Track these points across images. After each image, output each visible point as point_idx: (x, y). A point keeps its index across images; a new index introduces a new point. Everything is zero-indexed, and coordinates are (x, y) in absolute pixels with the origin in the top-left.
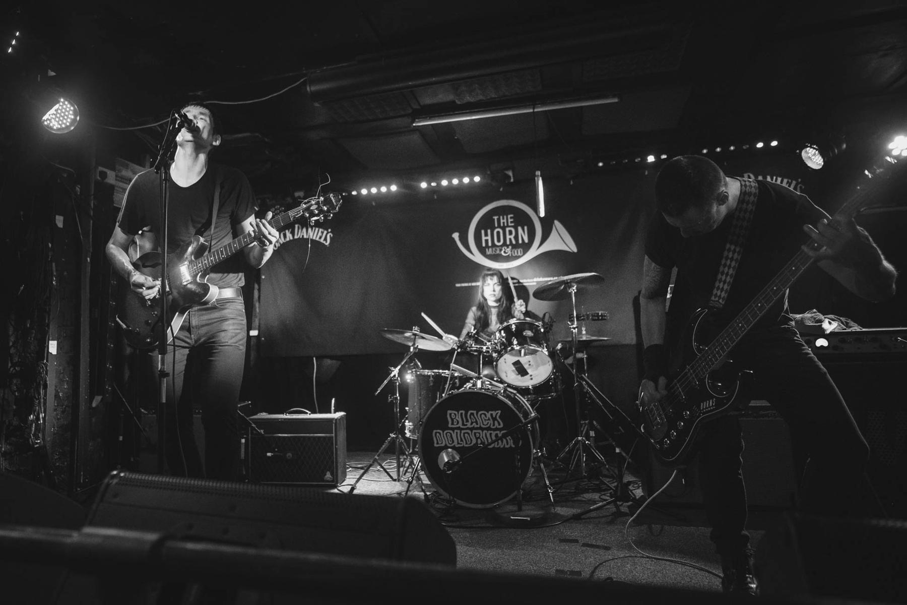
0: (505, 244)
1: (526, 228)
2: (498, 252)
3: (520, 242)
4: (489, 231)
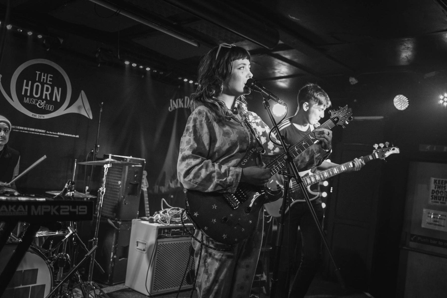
0: (41, 98)
1: (60, 89)
2: (34, 103)
3: (54, 99)
4: (30, 82)
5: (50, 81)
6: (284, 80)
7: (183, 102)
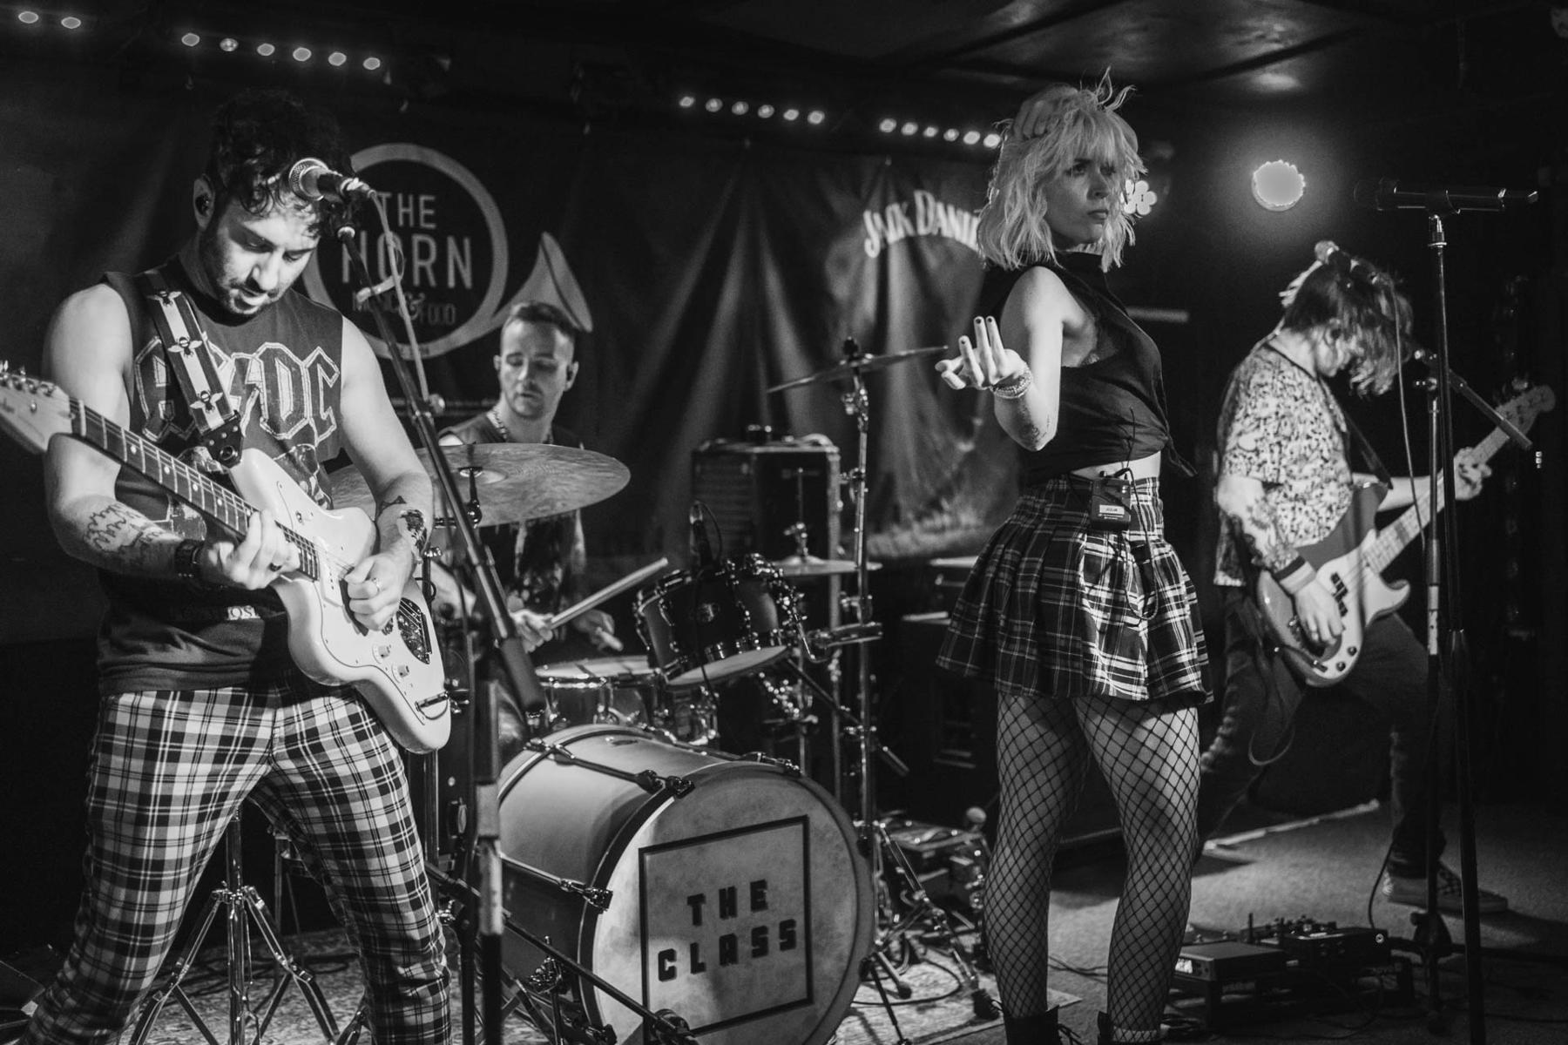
1: (467, 242)
3: (451, 283)
5: (428, 219)
6: (1276, 66)
7: (911, 213)
